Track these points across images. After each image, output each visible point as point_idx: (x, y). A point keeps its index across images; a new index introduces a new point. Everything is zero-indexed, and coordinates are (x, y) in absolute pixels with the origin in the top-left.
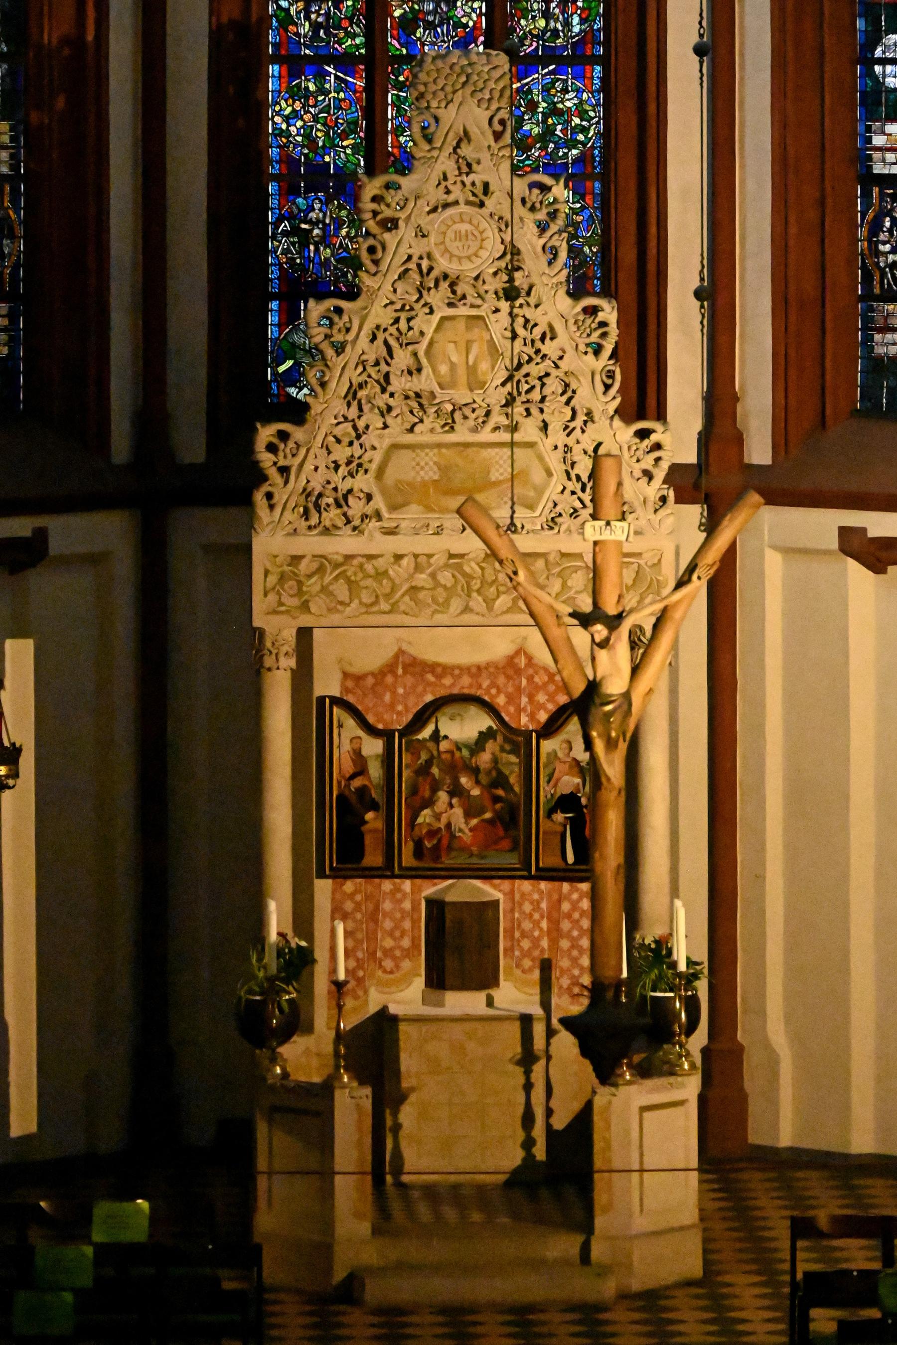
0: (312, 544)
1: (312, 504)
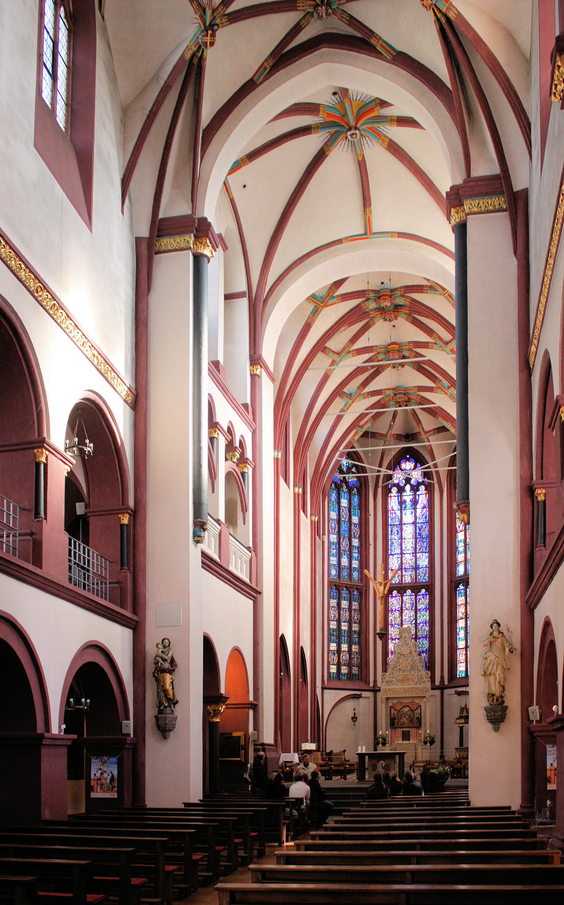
1: (387, 682)
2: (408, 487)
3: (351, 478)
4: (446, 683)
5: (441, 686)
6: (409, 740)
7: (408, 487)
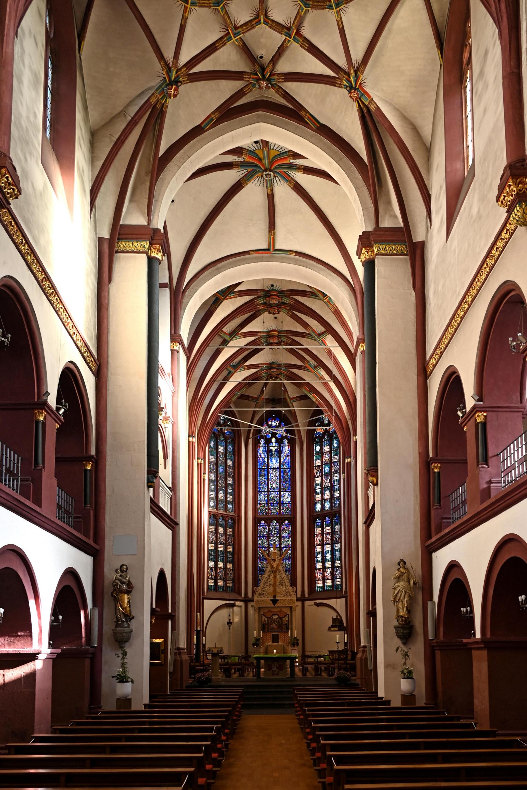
0: (260, 599)
1: (260, 594)
2: (274, 440)
3: (227, 430)
4: (306, 596)
5: (303, 599)
6: (278, 642)
7: (274, 440)
